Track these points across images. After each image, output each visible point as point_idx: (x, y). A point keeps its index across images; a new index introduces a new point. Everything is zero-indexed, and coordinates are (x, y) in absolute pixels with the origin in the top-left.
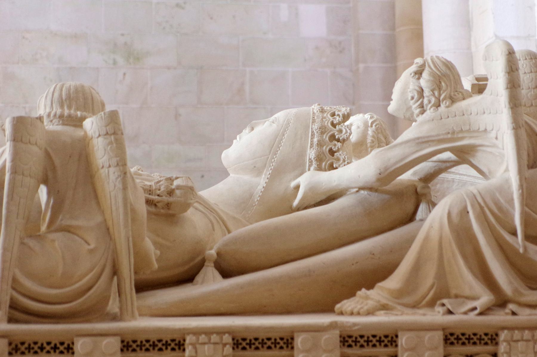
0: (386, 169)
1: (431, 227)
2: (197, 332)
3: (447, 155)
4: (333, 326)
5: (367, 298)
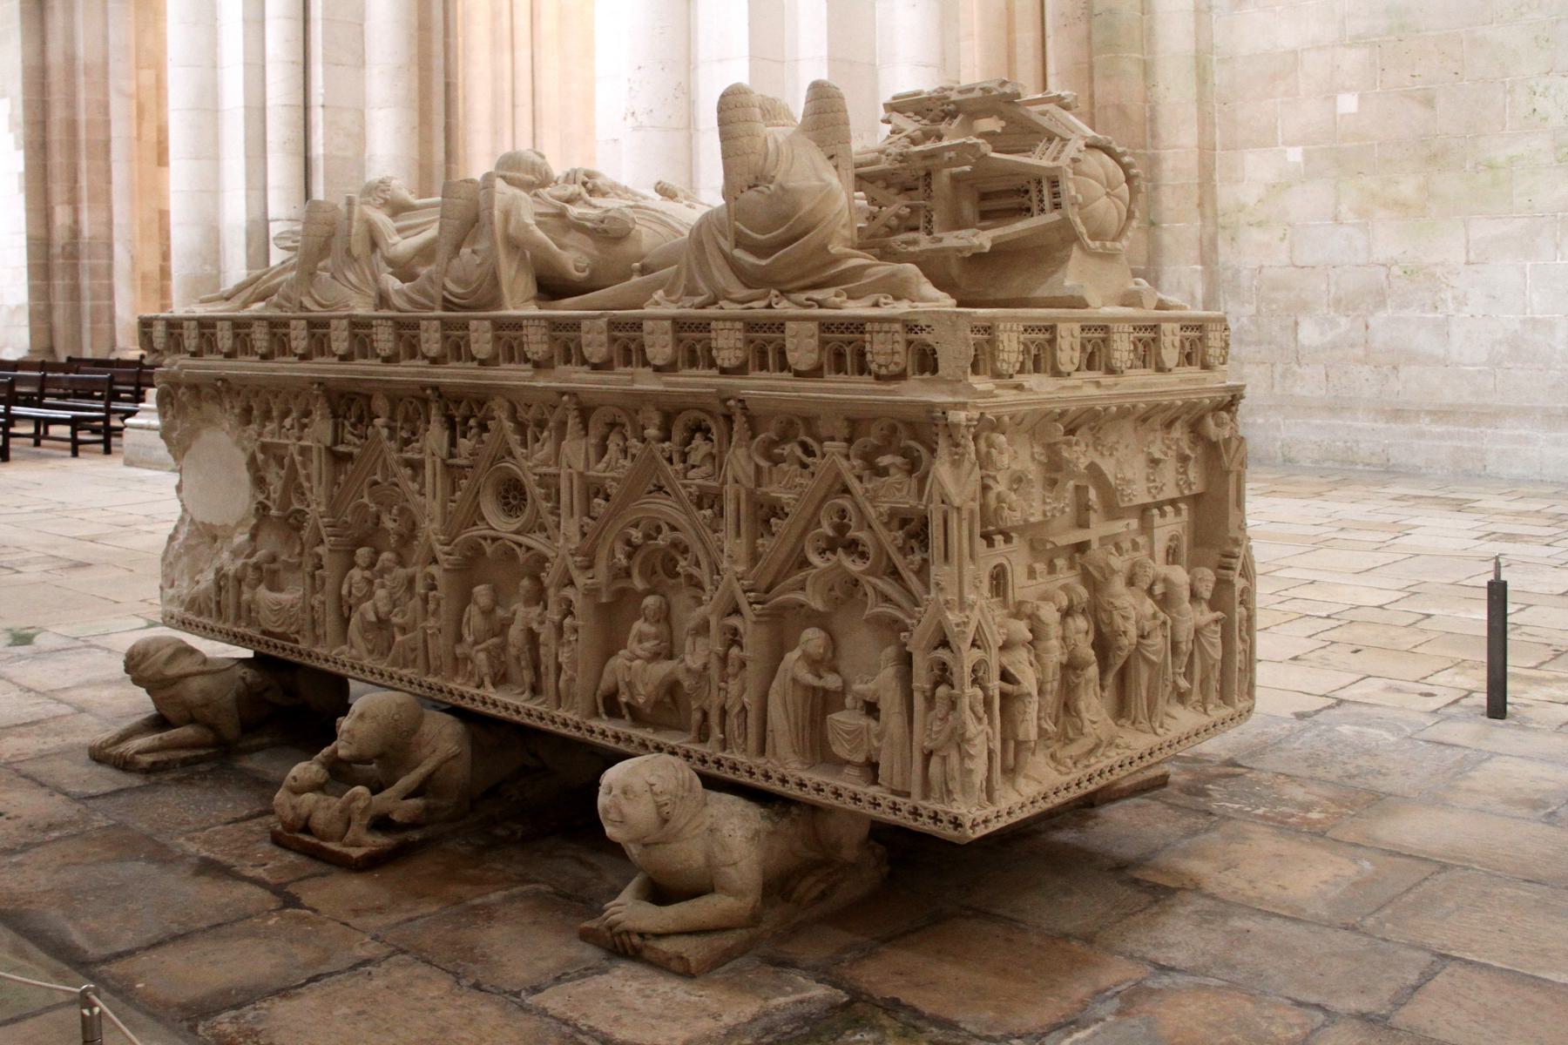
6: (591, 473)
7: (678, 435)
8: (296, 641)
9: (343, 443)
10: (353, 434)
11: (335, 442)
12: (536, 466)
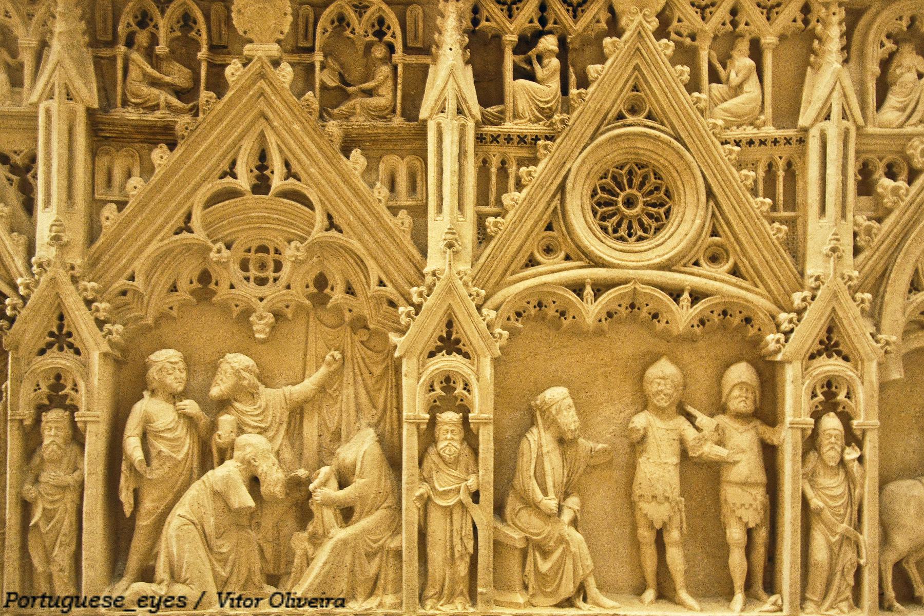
6: (870, 129)
9: (125, 103)
10: (155, 83)
12: (728, 127)
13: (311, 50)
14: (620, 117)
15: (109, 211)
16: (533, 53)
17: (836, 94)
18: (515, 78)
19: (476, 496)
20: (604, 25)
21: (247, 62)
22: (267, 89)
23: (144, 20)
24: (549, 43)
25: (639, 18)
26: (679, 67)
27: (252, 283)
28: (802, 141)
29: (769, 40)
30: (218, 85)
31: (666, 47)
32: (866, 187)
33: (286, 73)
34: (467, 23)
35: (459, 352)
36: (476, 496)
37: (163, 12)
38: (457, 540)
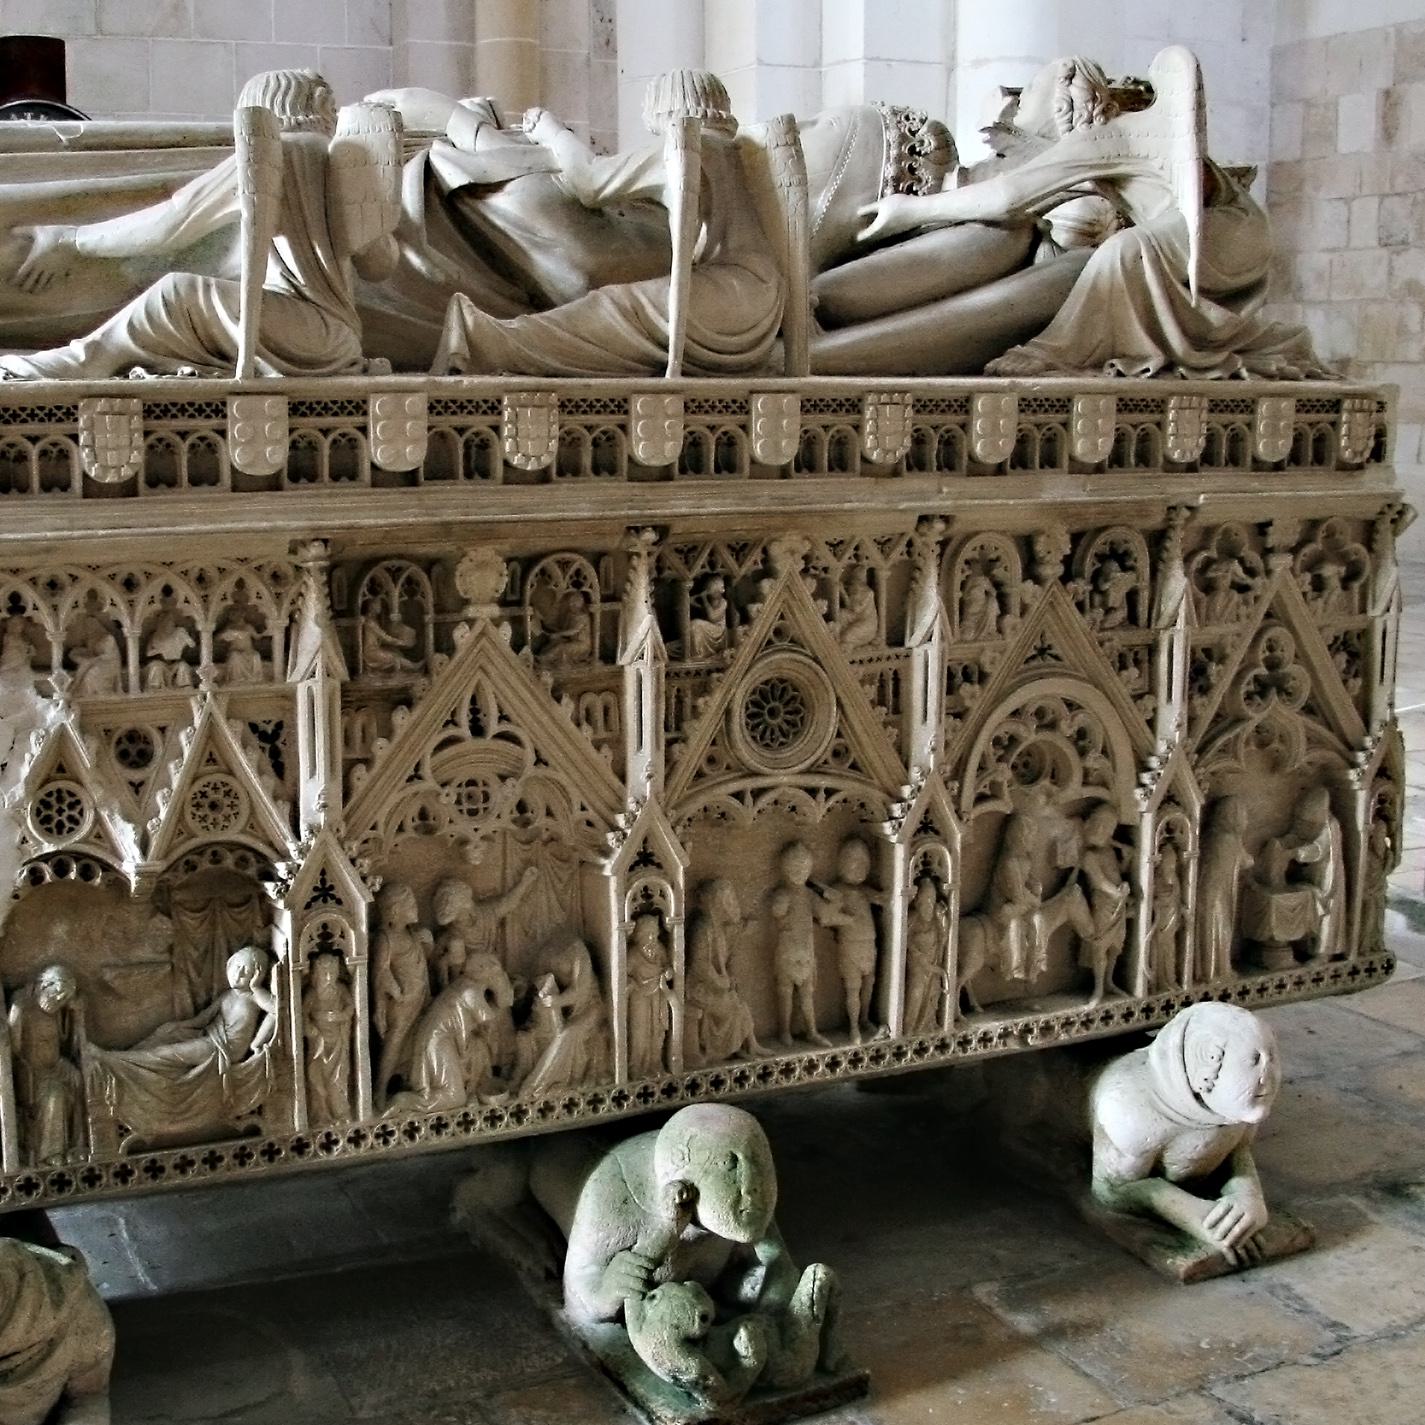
0: (1021, 199)
1: (1098, 274)
2: (879, 391)
3: (1088, 186)
4: (1012, 388)
5: (1026, 357)
7: (1089, 566)
8: (254, 1131)
10: (385, 646)
11: (353, 671)
13: (519, 603)
14: (770, 642)
15: (360, 771)
16: (704, 594)
17: (937, 622)
18: (693, 617)
19: (670, 984)
20: (760, 566)
21: (471, 622)
22: (488, 645)
23: (375, 588)
24: (718, 586)
25: (790, 561)
26: (820, 602)
27: (466, 816)
28: (907, 656)
29: (884, 575)
30: (446, 646)
31: (809, 586)
32: (951, 688)
33: (506, 632)
34: (655, 574)
35: (653, 863)
36: (670, 984)
37: (395, 581)
38: (656, 1021)
